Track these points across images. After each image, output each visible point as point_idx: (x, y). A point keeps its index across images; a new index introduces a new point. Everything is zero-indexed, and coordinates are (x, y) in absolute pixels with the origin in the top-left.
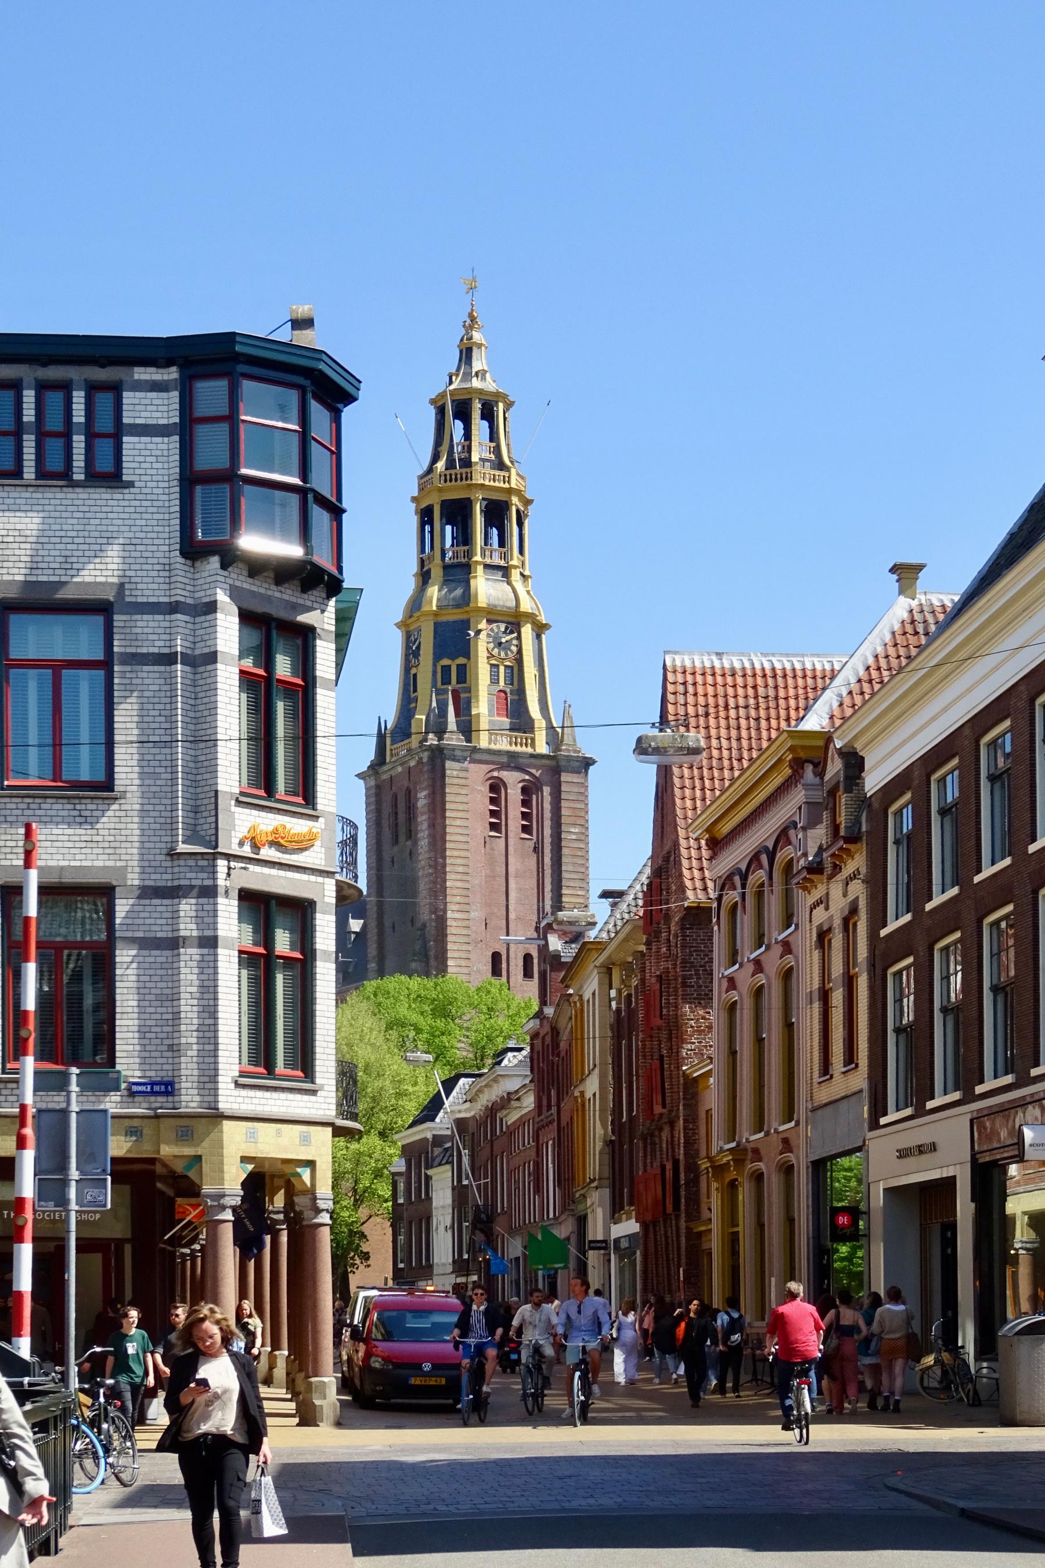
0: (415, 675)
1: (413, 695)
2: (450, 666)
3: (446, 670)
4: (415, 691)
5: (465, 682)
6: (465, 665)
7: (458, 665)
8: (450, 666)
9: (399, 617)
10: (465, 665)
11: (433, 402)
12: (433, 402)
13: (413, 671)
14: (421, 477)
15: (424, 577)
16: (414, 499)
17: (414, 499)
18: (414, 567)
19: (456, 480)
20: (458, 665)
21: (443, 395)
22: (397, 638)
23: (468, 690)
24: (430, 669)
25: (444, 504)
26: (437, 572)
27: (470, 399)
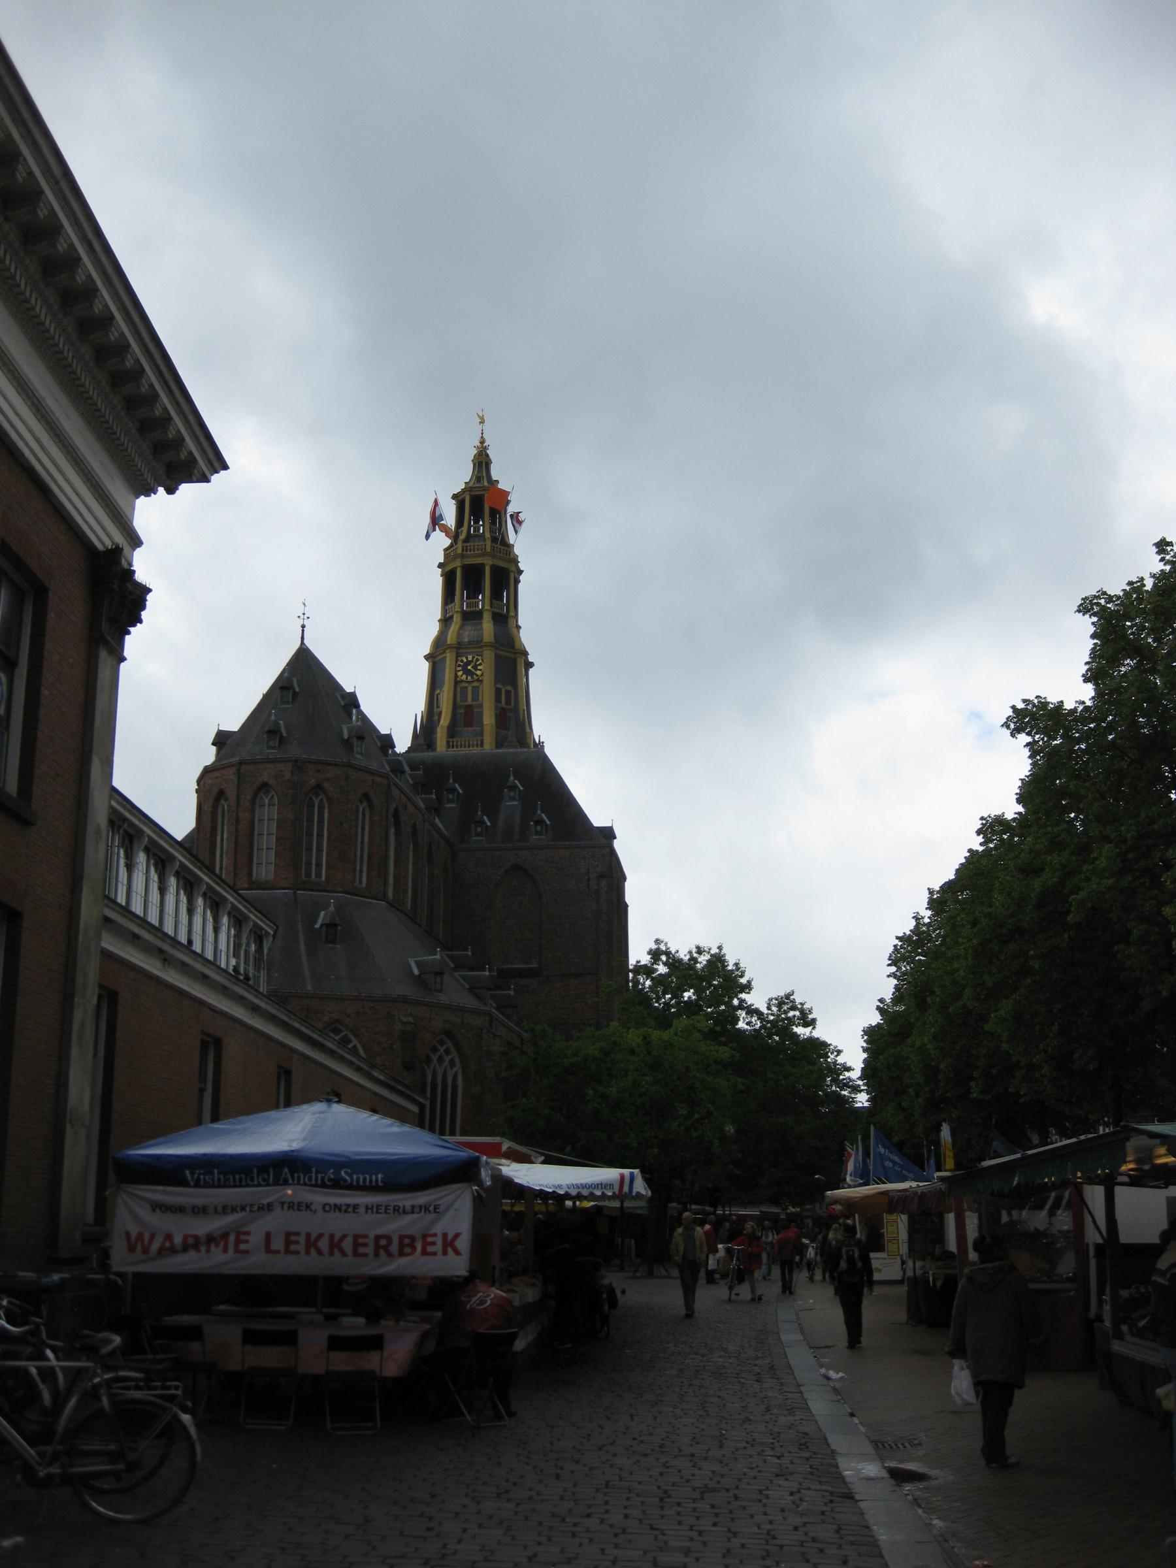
0: (437, 695)
1: (436, 710)
2: (467, 687)
4: (438, 707)
5: (477, 700)
6: (478, 687)
7: (473, 687)
8: (467, 687)
9: (427, 651)
10: (478, 687)
11: (455, 497)
12: (455, 497)
13: (438, 691)
14: (446, 550)
15: (445, 621)
16: (440, 566)
17: (440, 566)
18: (438, 615)
19: (474, 551)
20: (473, 687)
21: (463, 491)
22: (425, 666)
23: (481, 706)
25: (464, 567)
26: (457, 619)
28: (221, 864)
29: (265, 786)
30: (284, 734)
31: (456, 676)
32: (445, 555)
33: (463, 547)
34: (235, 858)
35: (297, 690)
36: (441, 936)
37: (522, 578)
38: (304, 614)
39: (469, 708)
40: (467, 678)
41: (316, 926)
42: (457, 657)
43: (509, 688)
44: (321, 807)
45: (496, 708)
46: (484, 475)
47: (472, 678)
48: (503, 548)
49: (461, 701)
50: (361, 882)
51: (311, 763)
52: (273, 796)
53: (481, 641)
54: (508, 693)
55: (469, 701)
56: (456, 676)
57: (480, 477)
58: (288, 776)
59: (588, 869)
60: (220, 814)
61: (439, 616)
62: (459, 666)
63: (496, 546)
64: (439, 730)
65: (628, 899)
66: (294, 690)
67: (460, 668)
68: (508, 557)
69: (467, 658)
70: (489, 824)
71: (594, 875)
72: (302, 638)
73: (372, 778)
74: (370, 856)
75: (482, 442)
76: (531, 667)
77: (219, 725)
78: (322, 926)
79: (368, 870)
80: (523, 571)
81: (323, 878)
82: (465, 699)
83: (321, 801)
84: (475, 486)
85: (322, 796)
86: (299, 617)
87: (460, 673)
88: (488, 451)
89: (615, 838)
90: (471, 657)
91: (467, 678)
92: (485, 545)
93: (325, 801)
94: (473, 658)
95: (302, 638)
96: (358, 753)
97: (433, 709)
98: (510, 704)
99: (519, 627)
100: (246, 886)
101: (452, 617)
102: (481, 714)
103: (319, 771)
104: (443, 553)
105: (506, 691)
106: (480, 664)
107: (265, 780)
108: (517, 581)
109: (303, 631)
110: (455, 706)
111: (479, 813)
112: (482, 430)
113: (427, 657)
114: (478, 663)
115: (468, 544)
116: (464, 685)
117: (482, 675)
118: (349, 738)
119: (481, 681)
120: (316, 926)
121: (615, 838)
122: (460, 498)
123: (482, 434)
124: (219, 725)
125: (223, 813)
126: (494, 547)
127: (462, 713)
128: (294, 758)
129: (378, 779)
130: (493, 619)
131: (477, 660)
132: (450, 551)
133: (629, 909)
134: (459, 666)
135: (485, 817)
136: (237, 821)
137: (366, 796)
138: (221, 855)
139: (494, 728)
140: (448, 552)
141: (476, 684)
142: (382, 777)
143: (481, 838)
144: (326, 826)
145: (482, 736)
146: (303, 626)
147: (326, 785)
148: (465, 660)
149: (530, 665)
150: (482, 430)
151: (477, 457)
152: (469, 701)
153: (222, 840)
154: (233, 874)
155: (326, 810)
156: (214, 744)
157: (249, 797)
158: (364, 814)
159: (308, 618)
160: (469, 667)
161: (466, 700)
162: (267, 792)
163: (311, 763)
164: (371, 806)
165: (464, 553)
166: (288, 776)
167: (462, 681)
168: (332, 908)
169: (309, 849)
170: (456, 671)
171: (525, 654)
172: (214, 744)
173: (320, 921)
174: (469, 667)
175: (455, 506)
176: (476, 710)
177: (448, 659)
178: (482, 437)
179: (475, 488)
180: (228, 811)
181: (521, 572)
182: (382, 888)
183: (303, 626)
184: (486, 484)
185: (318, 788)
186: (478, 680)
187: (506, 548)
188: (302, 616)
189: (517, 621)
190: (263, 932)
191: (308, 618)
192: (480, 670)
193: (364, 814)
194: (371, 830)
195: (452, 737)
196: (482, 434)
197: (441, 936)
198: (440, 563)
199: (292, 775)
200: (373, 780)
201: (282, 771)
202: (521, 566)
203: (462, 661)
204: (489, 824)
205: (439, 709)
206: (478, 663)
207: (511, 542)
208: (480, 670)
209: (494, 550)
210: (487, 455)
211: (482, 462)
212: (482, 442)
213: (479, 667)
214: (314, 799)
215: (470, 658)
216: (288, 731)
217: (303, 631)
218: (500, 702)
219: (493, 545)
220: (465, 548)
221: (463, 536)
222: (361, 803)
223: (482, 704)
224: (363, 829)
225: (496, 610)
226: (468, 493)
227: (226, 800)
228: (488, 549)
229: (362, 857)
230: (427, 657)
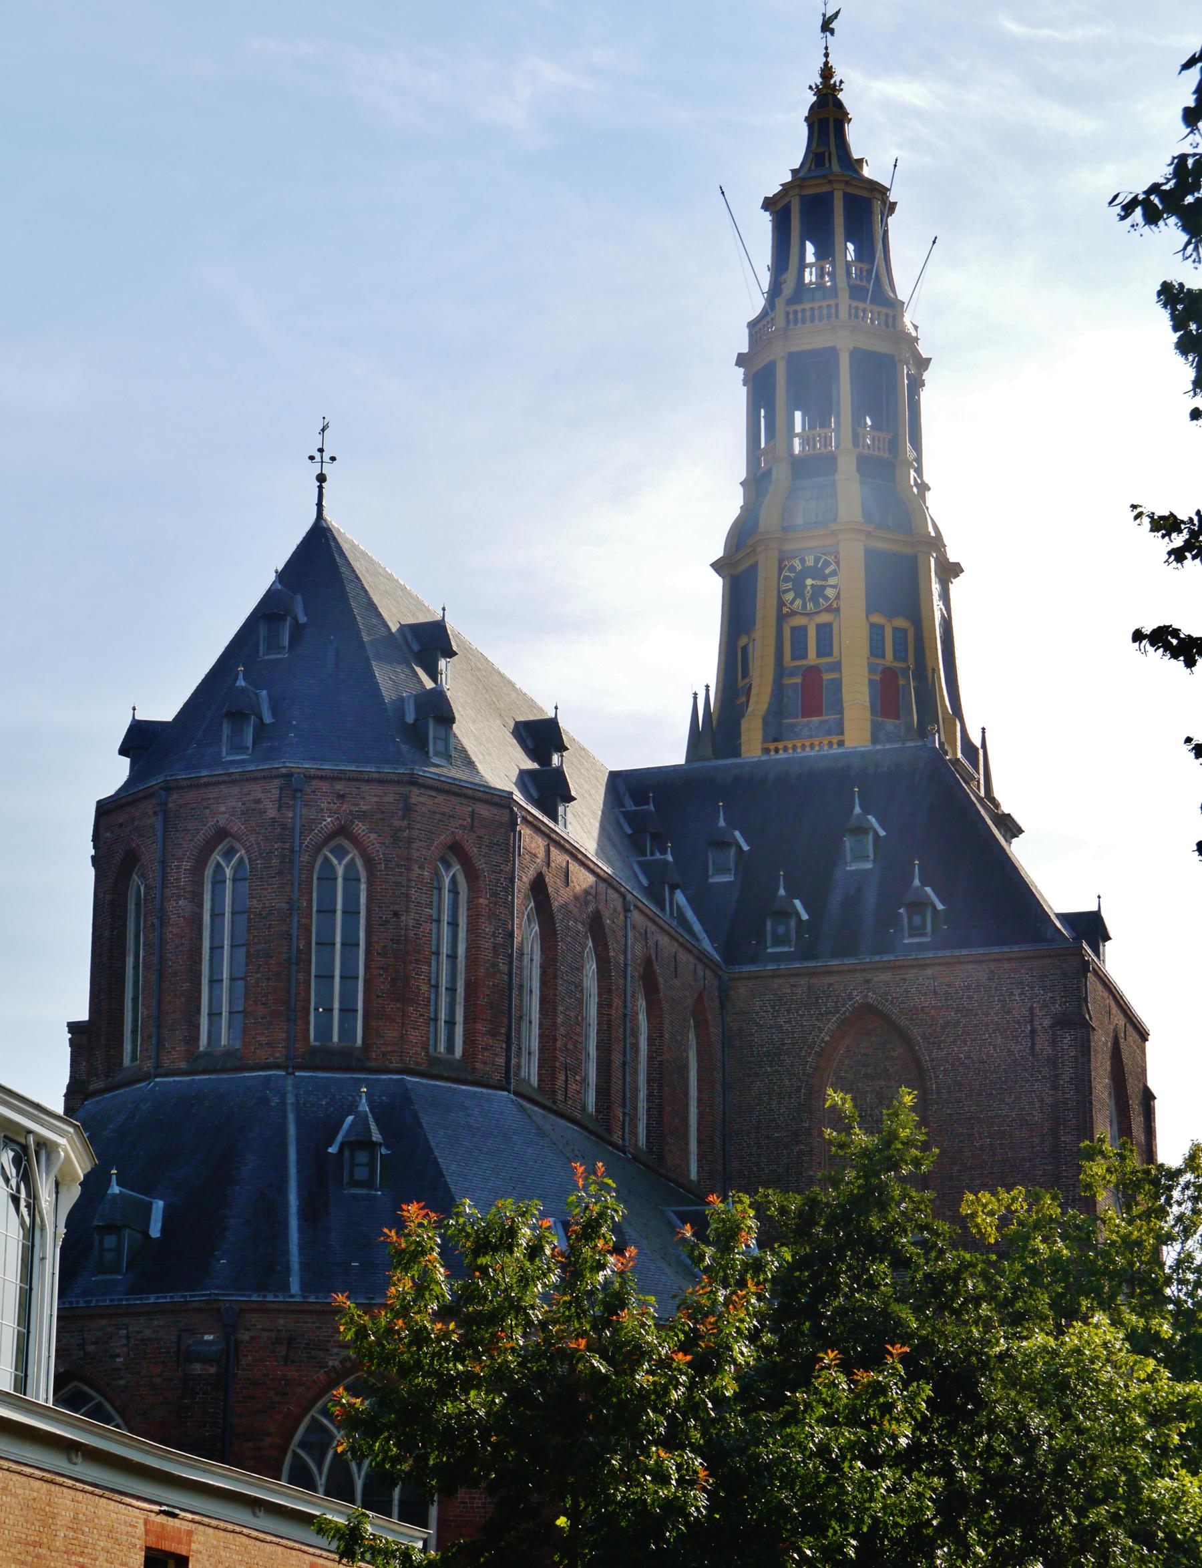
0: (745, 649)
1: (741, 683)
2: (804, 629)
3: (799, 634)
4: (745, 674)
5: (830, 654)
6: (829, 625)
8: (804, 629)
9: (718, 553)
10: (829, 625)
11: (768, 204)
12: (768, 204)
13: (743, 641)
14: (752, 325)
16: (741, 360)
17: (741, 360)
20: (818, 626)
22: (716, 584)
23: (837, 667)
24: (772, 631)
27: (831, 193)
28: (135, 1021)
29: (222, 834)
30: (268, 719)
31: (781, 603)
32: (751, 335)
33: (788, 313)
34: (160, 1001)
35: (303, 619)
36: (694, 1175)
37: (926, 376)
38: (321, 450)
39: (812, 674)
40: (804, 606)
41: (330, 1150)
42: (781, 561)
43: (901, 623)
44: (351, 879)
45: (872, 669)
46: (833, 149)
47: (817, 604)
48: (877, 309)
49: (794, 658)
50: (450, 1047)
51: (321, 778)
52: (241, 860)
53: (835, 520)
54: (899, 634)
55: (812, 657)
56: (781, 603)
57: (823, 154)
58: (271, 813)
59: (1031, 1009)
60: (131, 906)
61: (743, 476)
62: (787, 579)
63: (861, 305)
64: (744, 725)
65: (1154, 1082)
66: (296, 619)
67: (790, 585)
68: (891, 329)
69: (803, 561)
70: (805, 916)
71: (1046, 1023)
72: (320, 505)
73: (470, 809)
74: (471, 988)
75: (827, 72)
76: (957, 576)
77: (134, 709)
78: (342, 1145)
79: (466, 1020)
80: (929, 360)
81: (359, 1042)
82: (800, 651)
83: (351, 866)
84: (813, 174)
85: (353, 854)
86: (312, 458)
87: (789, 596)
88: (840, 96)
89: (1107, 938)
90: (812, 558)
91: (804, 606)
92: (837, 306)
93: (359, 863)
94: (817, 560)
95: (320, 505)
96: (437, 754)
97: (736, 683)
98: (905, 660)
99: (924, 487)
100: (183, 1065)
101: (768, 473)
102: (837, 685)
103: (341, 797)
104: (746, 331)
105: (895, 629)
106: (834, 574)
107: (222, 823)
108: (917, 384)
109: (320, 488)
110: (780, 671)
111: (782, 892)
112: (826, 48)
113: (717, 566)
114: (827, 571)
115: (799, 307)
116: (798, 621)
117: (838, 597)
118: (416, 720)
119: (838, 610)
120: (330, 1150)
121: (1107, 938)
122: (780, 206)
123: (826, 55)
124: (134, 709)
125: (138, 904)
126: (857, 308)
127: (797, 684)
128: (284, 771)
129: (484, 811)
130: (859, 469)
131: (827, 564)
132: (760, 325)
133: (1158, 1105)
134: (787, 579)
135: (797, 903)
136: (163, 921)
137: (456, 850)
138: (135, 1000)
139: (868, 715)
140: (757, 329)
141: (825, 618)
142: (495, 804)
143: (786, 949)
144: (363, 922)
145: (842, 733)
146: (321, 478)
147: (360, 828)
148: (799, 568)
149: (950, 571)
150: (826, 48)
151: (816, 109)
152: (812, 657)
153: (136, 967)
154: (154, 1040)
155: (363, 887)
156: (123, 751)
157: (186, 865)
158: (454, 891)
159: (333, 459)
160: (809, 582)
161: (805, 657)
162: (229, 854)
163: (321, 778)
164: (471, 874)
165: (791, 326)
166: (271, 813)
167: (793, 613)
168: (364, 1106)
169: (326, 977)
170: (780, 594)
171: (937, 543)
172: (123, 751)
173: (340, 1138)
174: (809, 582)
175: (770, 224)
176: (827, 677)
177: (761, 567)
178: (826, 63)
179: (811, 178)
180: (145, 900)
181: (924, 363)
182: (501, 1061)
183: (321, 478)
184: (836, 167)
185: (343, 831)
186: (829, 609)
187: (884, 311)
188: (317, 455)
189: (919, 471)
190: (31, 1138)
191: (333, 459)
192: (834, 587)
193: (454, 891)
194: (472, 928)
195: (775, 740)
196: (826, 55)
197: (694, 1175)
198: (739, 354)
199: (279, 809)
200: (473, 814)
201: (258, 801)
202: (924, 350)
203: (792, 569)
204: (805, 916)
205: (747, 681)
206: (827, 571)
207: (902, 294)
208: (834, 587)
209: (856, 316)
210: (839, 105)
211: (828, 119)
212: (827, 72)
213: (831, 581)
214: (335, 861)
215: (810, 562)
216: (274, 710)
217: (320, 488)
218: (883, 656)
219: (854, 304)
220: (791, 316)
221: (788, 289)
222: (448, 866)
223: (840, 663)
224: (454, 924)
225: (866, 451)
226: (796, 191)
227: (143, 876)
228: (844, 313)
229: (452, 990)
230: (717, 566)
